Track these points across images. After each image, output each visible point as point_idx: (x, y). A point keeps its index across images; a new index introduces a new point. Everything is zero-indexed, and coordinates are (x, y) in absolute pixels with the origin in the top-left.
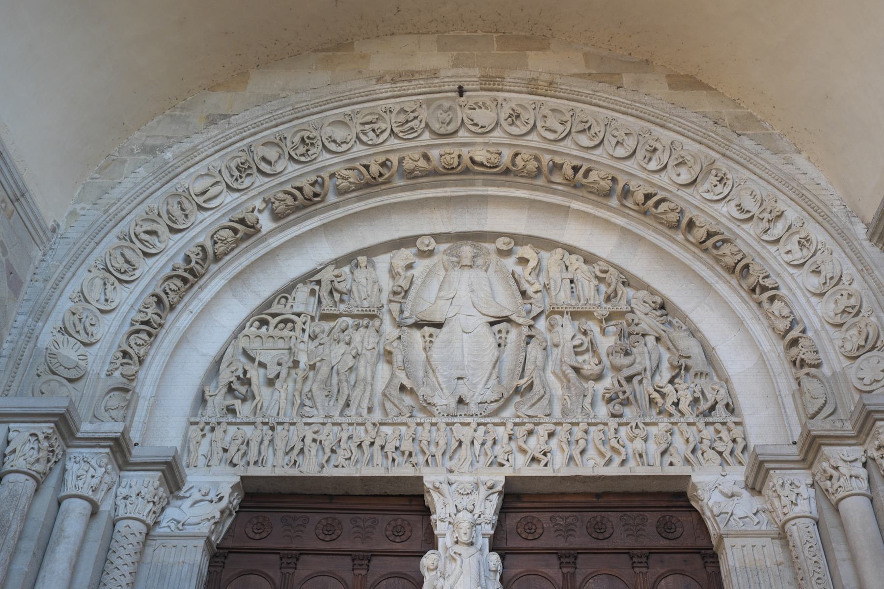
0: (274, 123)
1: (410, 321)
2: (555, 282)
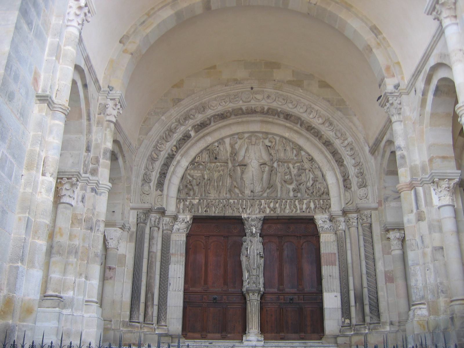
0: (194, 103)
1: (237, 165)
2: (280, 150)
